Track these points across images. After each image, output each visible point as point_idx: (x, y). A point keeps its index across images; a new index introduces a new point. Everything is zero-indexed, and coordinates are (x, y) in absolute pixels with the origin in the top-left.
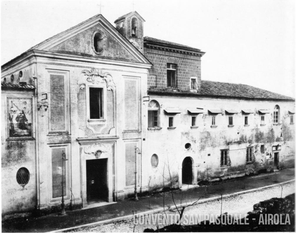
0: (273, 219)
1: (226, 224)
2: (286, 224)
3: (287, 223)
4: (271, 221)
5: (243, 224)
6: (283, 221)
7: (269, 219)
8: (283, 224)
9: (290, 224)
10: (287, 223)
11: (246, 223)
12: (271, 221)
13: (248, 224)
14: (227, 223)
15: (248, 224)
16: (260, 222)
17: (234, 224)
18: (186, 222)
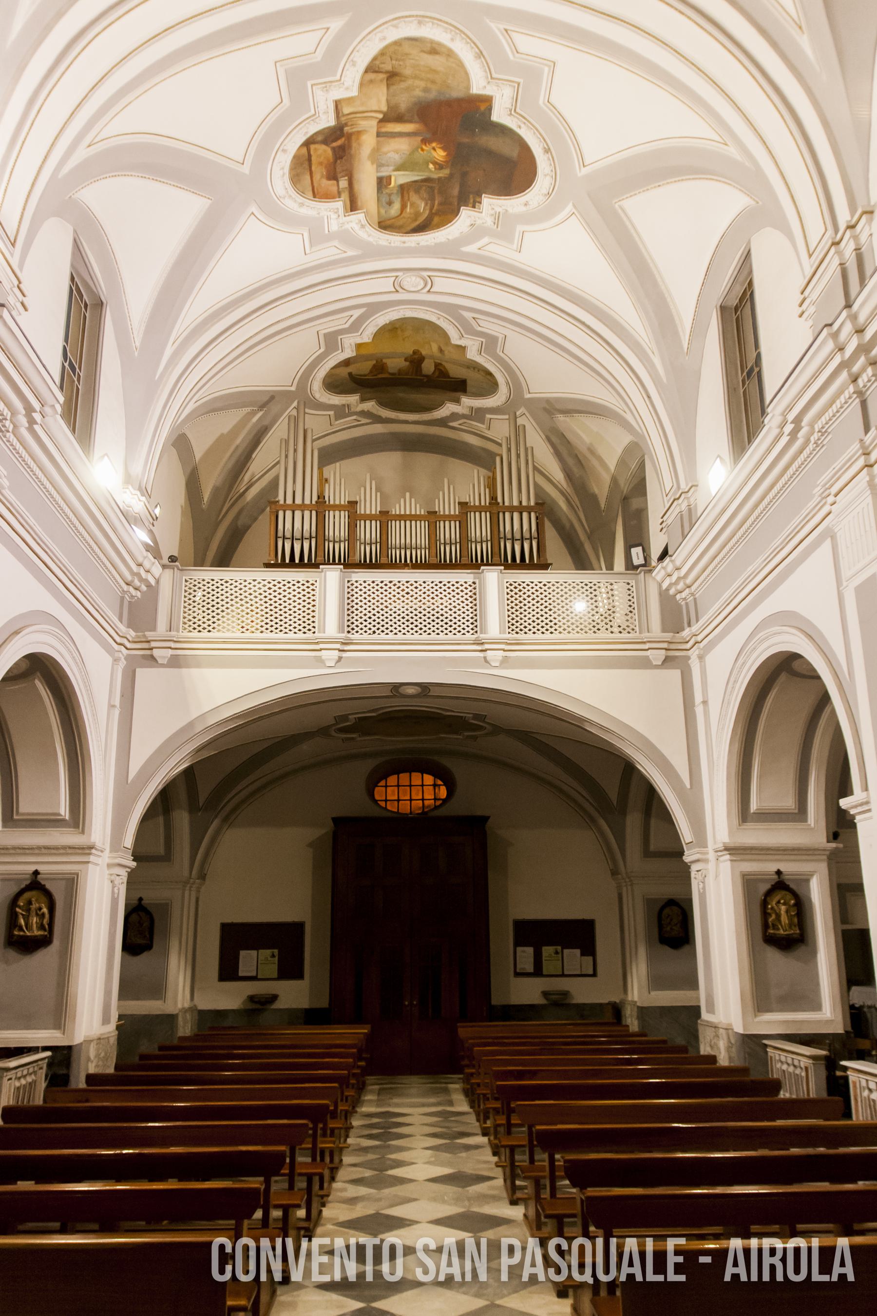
0: (784, 1260)
1: (591, 1281)
2: (835, 1278)
3: (843, 1277)
4: (773, 1268)
5: (660, 1278)
6: (826, 1268)
7: (767, 1260)
8: (825, 1278)
9: (851, 1278)
10: (843, 1277)
11: (672, 1277)
12: (773, 1268)
13: (682, 1278)
14: (594, 1275)
15: (682, 1278)
16: (729, 1271)
17: (623, 1278)
18: (426, 1272)
